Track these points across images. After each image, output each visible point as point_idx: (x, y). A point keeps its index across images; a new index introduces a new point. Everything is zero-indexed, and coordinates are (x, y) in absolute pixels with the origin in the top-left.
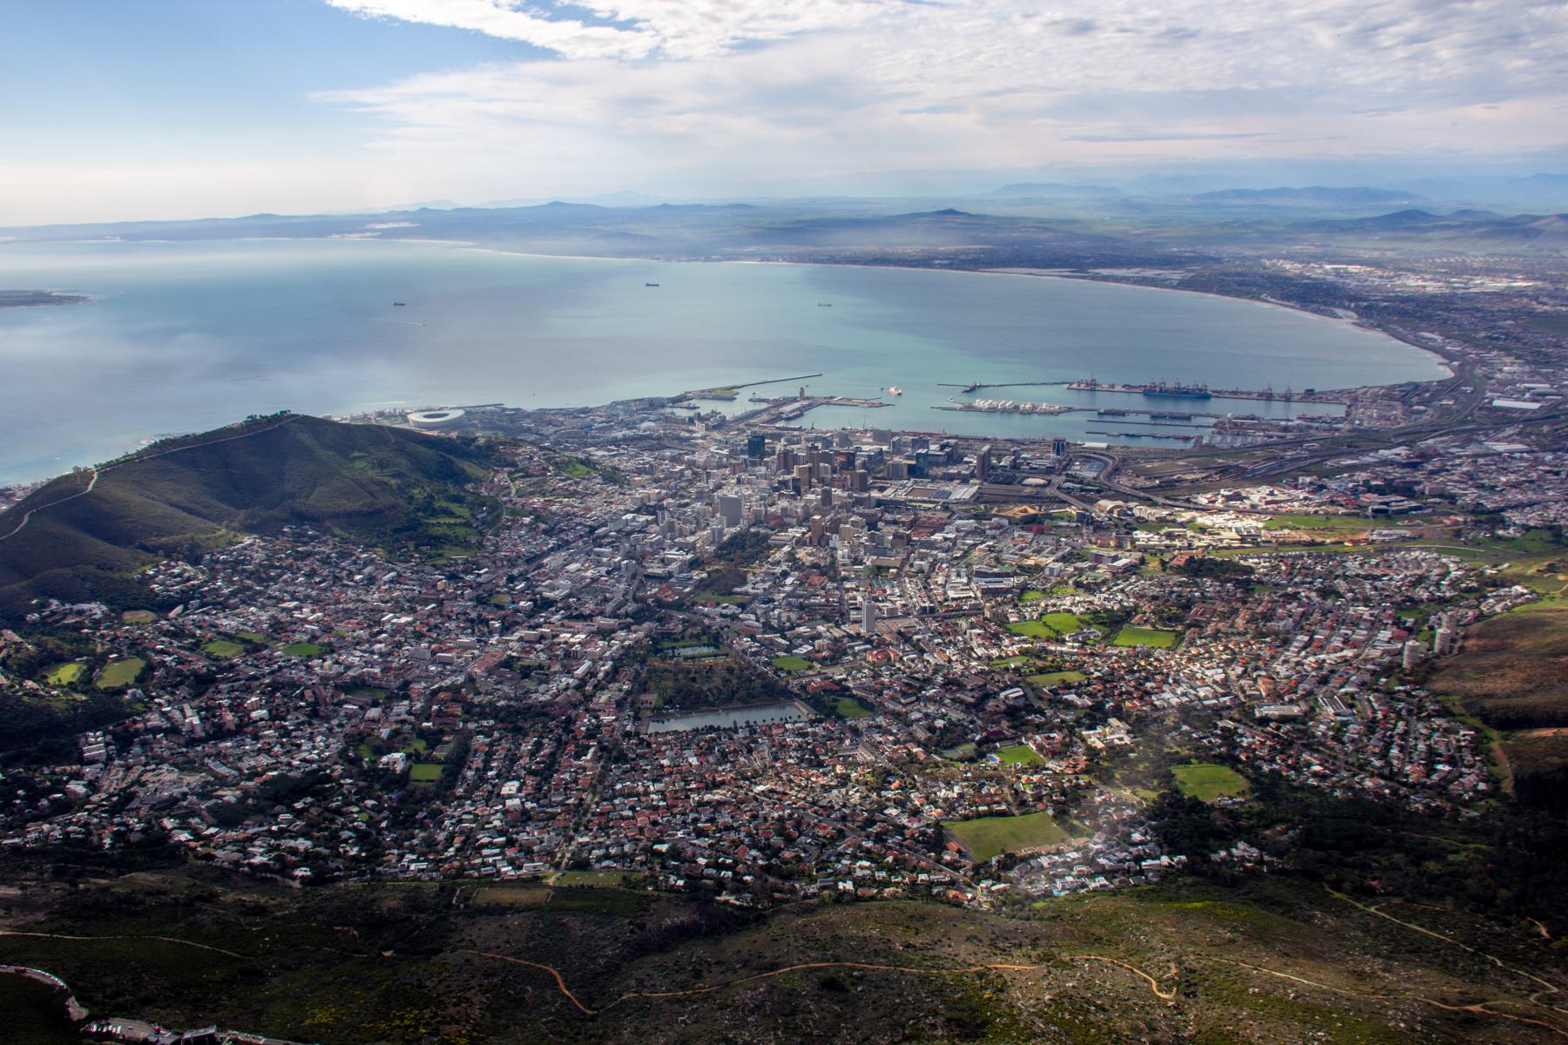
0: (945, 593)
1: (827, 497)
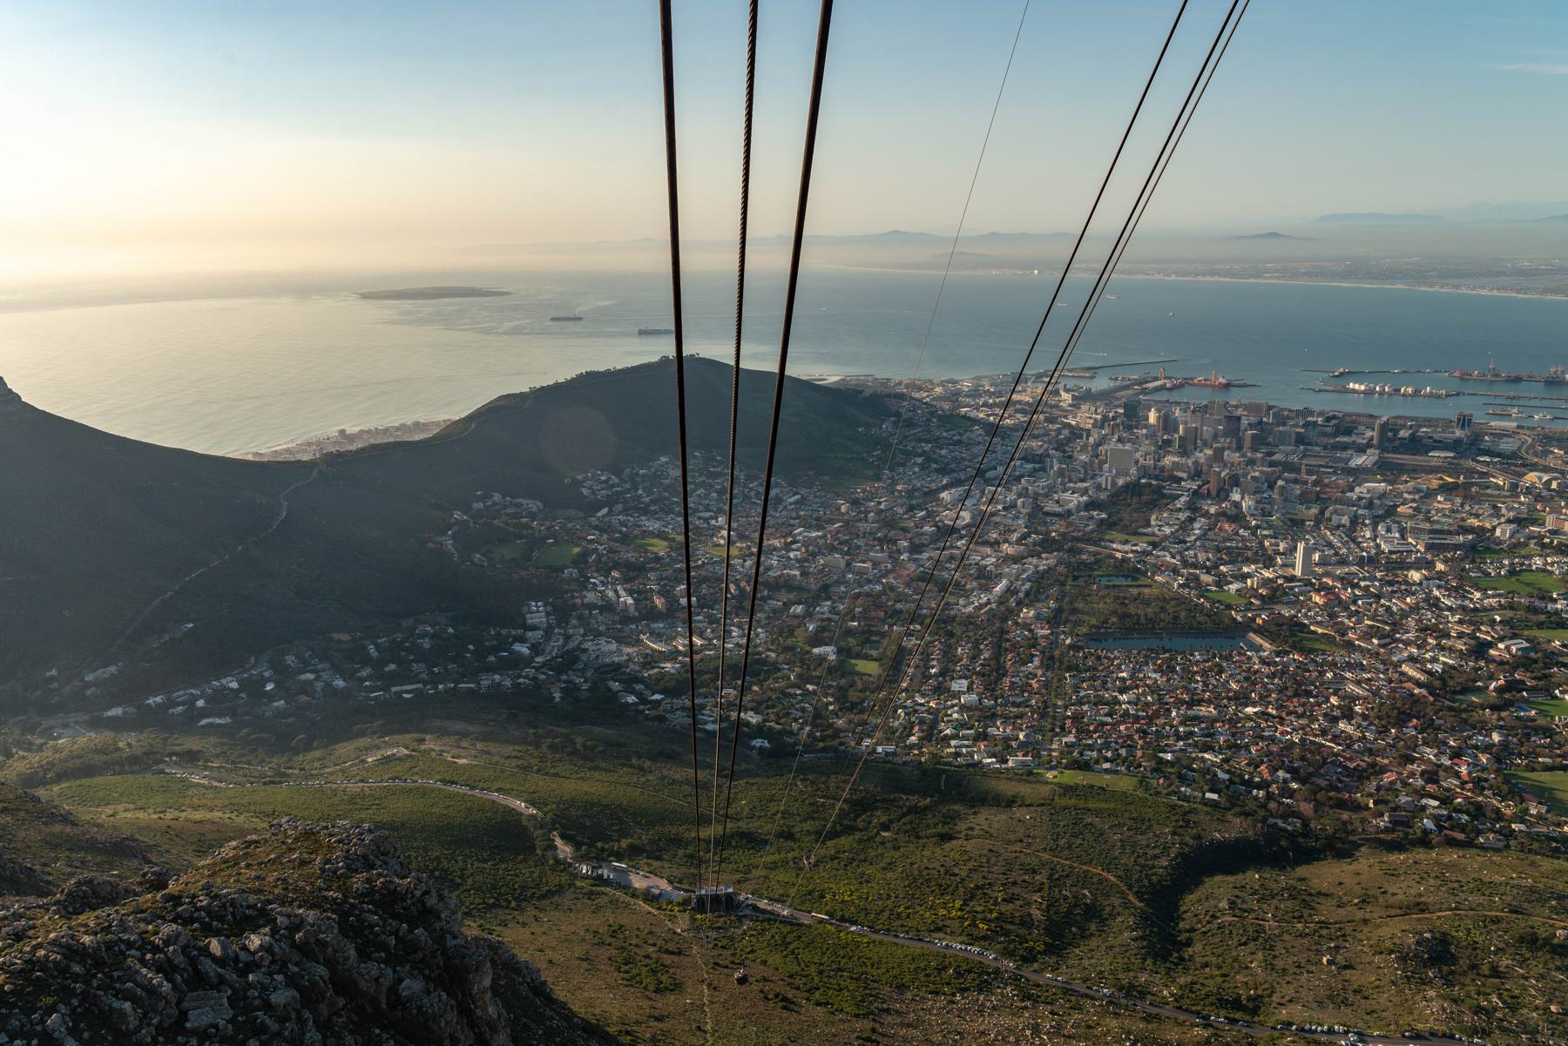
0: (1378, 546)
1: (1218, 456)
